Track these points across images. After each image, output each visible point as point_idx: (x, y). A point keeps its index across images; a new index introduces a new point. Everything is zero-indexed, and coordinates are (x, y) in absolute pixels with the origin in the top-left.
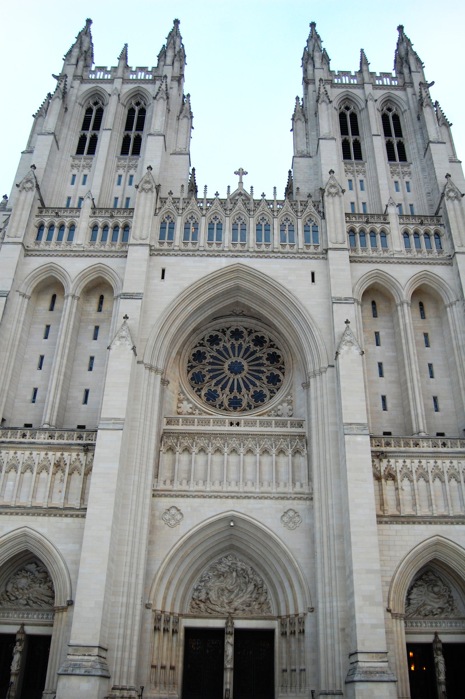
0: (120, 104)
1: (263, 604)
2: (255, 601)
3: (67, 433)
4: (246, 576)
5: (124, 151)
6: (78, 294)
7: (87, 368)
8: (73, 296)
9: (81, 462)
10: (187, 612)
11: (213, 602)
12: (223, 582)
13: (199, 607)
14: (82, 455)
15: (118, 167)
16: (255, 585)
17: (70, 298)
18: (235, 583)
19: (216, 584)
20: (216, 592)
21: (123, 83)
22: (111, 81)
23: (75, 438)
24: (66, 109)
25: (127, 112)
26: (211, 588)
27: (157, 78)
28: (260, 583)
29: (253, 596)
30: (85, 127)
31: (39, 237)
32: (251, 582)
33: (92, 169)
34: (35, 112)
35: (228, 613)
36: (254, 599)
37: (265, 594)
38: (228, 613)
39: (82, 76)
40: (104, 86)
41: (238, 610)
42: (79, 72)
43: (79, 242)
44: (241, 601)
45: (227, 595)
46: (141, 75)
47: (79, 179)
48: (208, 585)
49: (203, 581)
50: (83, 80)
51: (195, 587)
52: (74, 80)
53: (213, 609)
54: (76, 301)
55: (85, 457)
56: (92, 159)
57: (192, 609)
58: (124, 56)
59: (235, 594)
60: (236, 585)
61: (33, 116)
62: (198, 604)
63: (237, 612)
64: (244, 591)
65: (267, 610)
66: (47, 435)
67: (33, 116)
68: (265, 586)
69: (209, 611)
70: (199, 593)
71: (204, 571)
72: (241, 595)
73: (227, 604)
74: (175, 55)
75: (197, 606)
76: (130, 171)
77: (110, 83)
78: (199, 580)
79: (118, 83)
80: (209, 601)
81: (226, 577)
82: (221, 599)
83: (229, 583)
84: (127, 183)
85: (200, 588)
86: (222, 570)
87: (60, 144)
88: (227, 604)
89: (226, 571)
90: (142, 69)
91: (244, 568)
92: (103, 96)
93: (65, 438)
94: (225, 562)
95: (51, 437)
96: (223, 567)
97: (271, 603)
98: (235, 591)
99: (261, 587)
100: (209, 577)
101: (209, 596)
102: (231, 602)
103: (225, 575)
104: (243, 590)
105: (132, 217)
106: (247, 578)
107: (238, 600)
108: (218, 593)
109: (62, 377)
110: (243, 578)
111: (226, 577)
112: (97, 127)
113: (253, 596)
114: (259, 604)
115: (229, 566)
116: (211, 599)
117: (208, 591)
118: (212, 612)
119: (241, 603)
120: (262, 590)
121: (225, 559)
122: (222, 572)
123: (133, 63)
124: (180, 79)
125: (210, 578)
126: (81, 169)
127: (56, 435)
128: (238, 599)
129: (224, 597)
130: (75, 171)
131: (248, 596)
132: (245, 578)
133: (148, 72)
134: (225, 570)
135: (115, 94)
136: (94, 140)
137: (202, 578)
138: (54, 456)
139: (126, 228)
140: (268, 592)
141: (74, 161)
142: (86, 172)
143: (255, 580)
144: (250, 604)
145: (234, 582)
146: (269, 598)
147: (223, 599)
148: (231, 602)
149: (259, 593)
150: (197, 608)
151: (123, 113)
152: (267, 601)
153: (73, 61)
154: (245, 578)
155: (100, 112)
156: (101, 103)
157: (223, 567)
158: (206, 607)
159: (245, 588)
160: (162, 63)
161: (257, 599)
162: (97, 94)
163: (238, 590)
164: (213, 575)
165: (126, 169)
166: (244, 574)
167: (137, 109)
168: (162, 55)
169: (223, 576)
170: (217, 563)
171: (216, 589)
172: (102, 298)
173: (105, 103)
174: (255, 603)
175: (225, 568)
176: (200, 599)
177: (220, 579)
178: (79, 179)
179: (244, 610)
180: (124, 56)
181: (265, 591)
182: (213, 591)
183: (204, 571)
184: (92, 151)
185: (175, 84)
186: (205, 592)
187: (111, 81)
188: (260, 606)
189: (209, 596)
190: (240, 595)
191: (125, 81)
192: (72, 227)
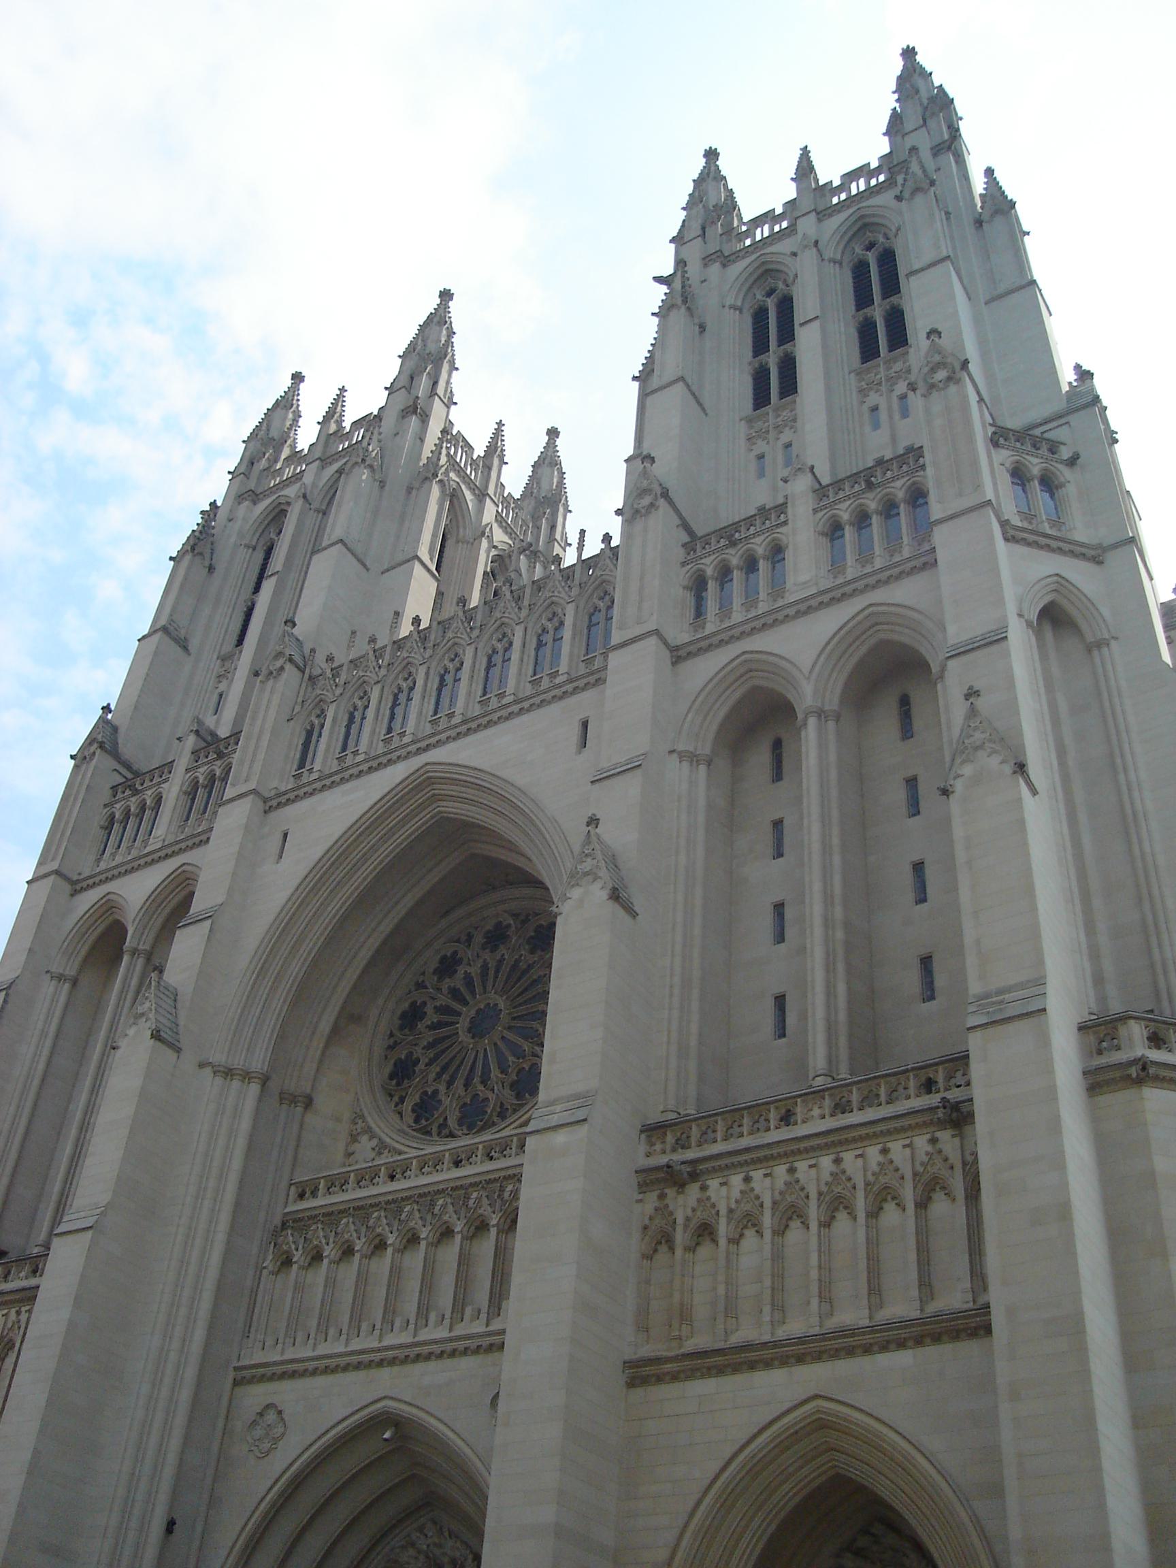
0: (826, 263)
3: (886, 1083)
6: (832, 702)
7: (910, 896)
8: (820, 714)
9: (946, 1160)
14: (945, 1136)
15: (863, 392)
17: (812, 721)
21: (820, 220)
22: (791, 230)
23: (912, 1091)
24: (702, 328)
27: (896, 169)
30: (760, 345)
31: (699, 612)
33: (798, 424)
34: (636, 369)
39: (720, 251)
40: (776, 248)
43: (804, 577)
50: (726, 260)
52: (706, 265)
54: (831, 725)
55: (957, 1140)
66: (828, 1103)
76: (895, 387)
77: (789, 235)
79: (807, 225)
84: (897, 416)
87: (707, 405)
92: (785, 269)
93: (883, 1098)
95: (841, 1108)
105: (923, 467)
109: (840, 935)
112: (787, 334)
123: (828, 172)
126: (772, 435)
127: (855, 1097)
130: (761, 446)
135: (806, 246)
136: (789, 366)
138: (860, 1160)
139: (918, 496)
141: (752, 427)
151: (843, 282)
155: (786, 306)
162: (767, 271)
165: (883, 388)
167: (871, 258)
168: (895, 127)
172: (905, 702)
180: (805, 168)
184: (789, 386)
191: (824, 213)
192: (777, 552)
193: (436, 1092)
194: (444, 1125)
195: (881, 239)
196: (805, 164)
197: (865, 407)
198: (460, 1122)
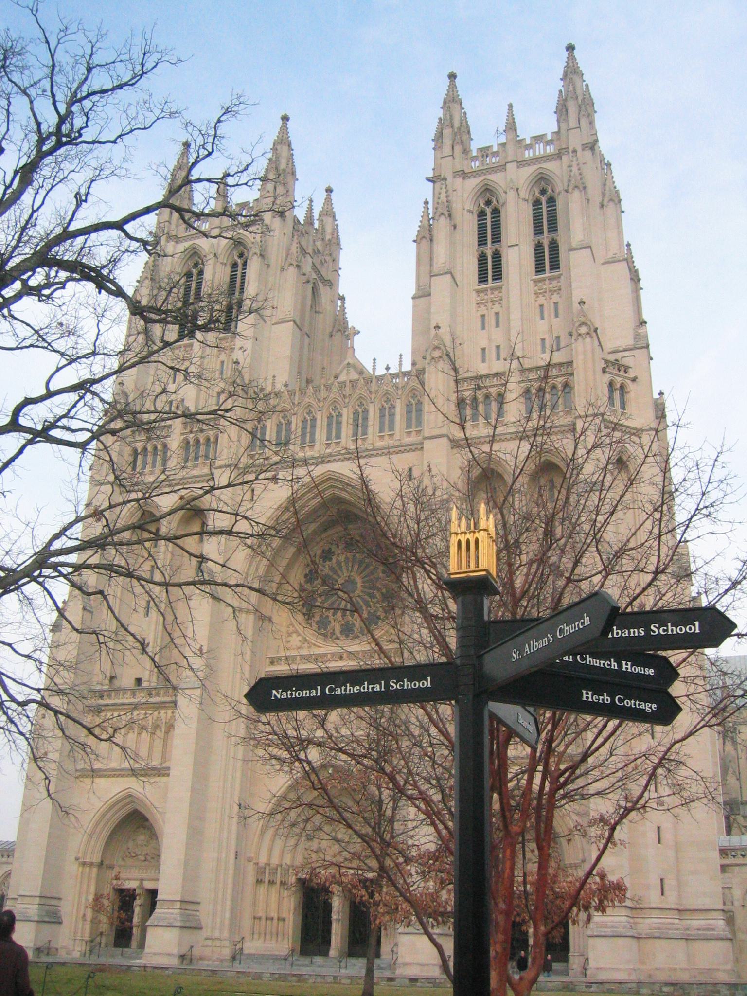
0: (521, 201)
5: (540, 268)
21: (518, 167)
25: (531, 207)
30: (482, 241)
33: (504, 302)
42: (458, 167)
46: (540, 150)
47: (491, 320)
52: (454, 177)
56: (500, 288)
58: (511, 126)
61: (415, 241)
67: (415, 241)
74: (579, 106)
84: (553, 315)
90: (539, 139)
123: (526, 133)
124: (592, 146)
126: (490, 304)
133: (549, 143)
142: (497, 308)
151: (527, 211)
153: (447, 150)
156: (495, 202)
160: (563, 125)
173: (501, 202)
178: (491, 320)
180: (511, 126)
185: (588, 153)
187: (502, 168)
191: (521, 164)
193: (328, 616)
194: (333, 633)
195: (550, 191)
196: (510, 118)
197: (537, 304)
198: (341, 633)
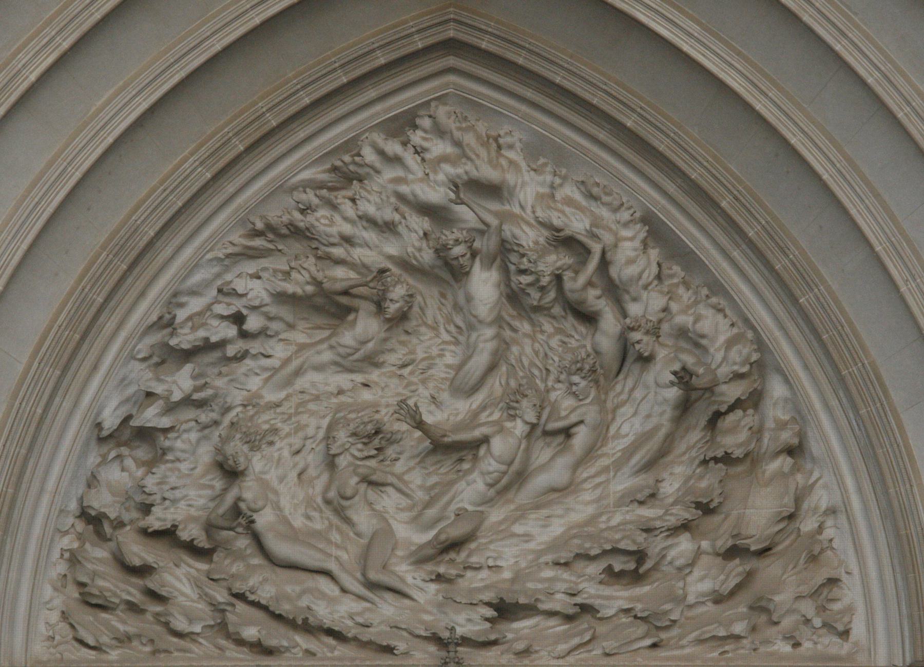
1: (764, 552)
2: (685, 527)
4: (594, 299)
10: (39, 649)
11: (282, 549)
12: (372, 361)
13: (154, 595)
16: (684, 377)
18: (492, 367)
19: (302, 383)
20: (312, 459)
26: (264, 420)
28: (740, 354)
29: (670, 487)
32: (646, 360)
35: (435, 639)
36: (682, 513)
37: (783, 463)
38: (435, 639)
41: (530, 610)
44: (557, 529)
45: (416, 478)
48: (237, 397)
49: (187, 355)
51: (110, 420)
53: (285, 608)
57: (87, 616)
59: (491, 465)
60: (496, 385)
62: (143, 571)
63: (524, 625)
64: (581, 437)
65: (807, 608)
68: (777, 389)
69: (250, 633)
70: (150, 465)
71: (193, 267)
72: (558, 473)
73: (421, 559)
75: (131, 590)
78: (143, 347)
80: (243, 543)
81: (403, 317)
82: (363, 519)
83: (439, 372)
85: (151, 416)
86: (358, 253)
88: (421, 559)
89: (405, 264)
91: (578, 225)
94: (389, 173)
96: (372, 222)
97: (843, 544)
98: (498, 445)
99: (737, 404)
100: (238, 319)
101: (249, 490)
102: (455, 545)
103: (398, 292)
104: (567, 432)
106: (610, 323)
107: (529, 526)
108: (331, 462)
110: (570, 323)
111: (403, 317)
113: (670, 487)
114: (733, 552)
115: (427, 210)
116: (264, 520)
117: (236, 448)
118: (277, 636)
119: (553, 546)
120: (757, 432)
121: (393, 147)
122: (361, 268)
125: (253, 323)
128: (521, 514)
129: (389, 501)
131: (622, 483)
132: (589, 318)
134: (392, 248)
137: (166, 323)
140: (815, 447)
143: (682, 333)
144: (640, 556)
145: (480, 361)
146: (821, 498)
147: (381, 516)
148: (455, 545)
149: (727, 459)
150: (133, 607)
152: (808, 525)
154: (589, 318)
157: (372, 222)
158: (221, 596)
159: (591, 414)
161: (706, 509)
163: (519, 428)
164: (281, 297)
166: (574, 284)
169: (380, 307)
170: (318, 186)
171: (315, 425)
174: (684, 545)
175: (388, 228)
176: (154, 522)
177: (348, 338)
179: (586, 609)
181: (787, 437)
182: (282, 448)
183: (193, 267)
186: (205, 454)
188: (737, 567)
189: (249, 490)
190: (540, 481)
